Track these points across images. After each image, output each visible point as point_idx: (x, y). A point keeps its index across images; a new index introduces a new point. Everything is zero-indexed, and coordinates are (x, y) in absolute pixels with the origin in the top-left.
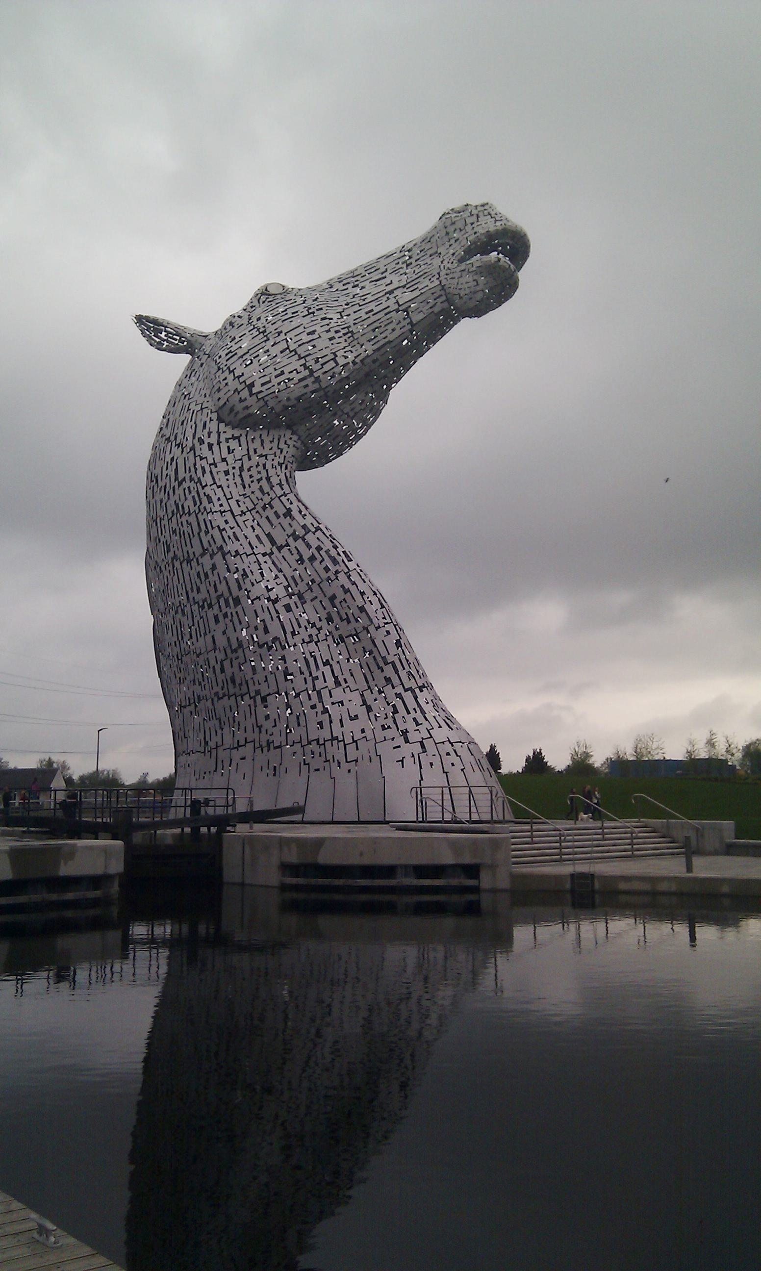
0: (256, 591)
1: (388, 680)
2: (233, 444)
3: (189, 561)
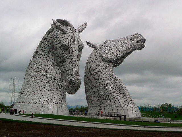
0: (109, 86)
1: (128, 99)
2: (104, 64)
3: (98, 80)
